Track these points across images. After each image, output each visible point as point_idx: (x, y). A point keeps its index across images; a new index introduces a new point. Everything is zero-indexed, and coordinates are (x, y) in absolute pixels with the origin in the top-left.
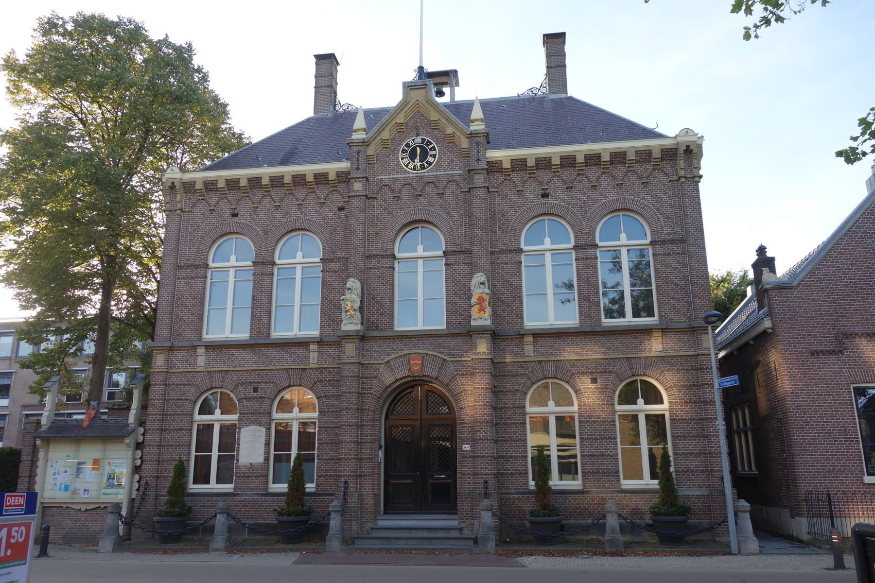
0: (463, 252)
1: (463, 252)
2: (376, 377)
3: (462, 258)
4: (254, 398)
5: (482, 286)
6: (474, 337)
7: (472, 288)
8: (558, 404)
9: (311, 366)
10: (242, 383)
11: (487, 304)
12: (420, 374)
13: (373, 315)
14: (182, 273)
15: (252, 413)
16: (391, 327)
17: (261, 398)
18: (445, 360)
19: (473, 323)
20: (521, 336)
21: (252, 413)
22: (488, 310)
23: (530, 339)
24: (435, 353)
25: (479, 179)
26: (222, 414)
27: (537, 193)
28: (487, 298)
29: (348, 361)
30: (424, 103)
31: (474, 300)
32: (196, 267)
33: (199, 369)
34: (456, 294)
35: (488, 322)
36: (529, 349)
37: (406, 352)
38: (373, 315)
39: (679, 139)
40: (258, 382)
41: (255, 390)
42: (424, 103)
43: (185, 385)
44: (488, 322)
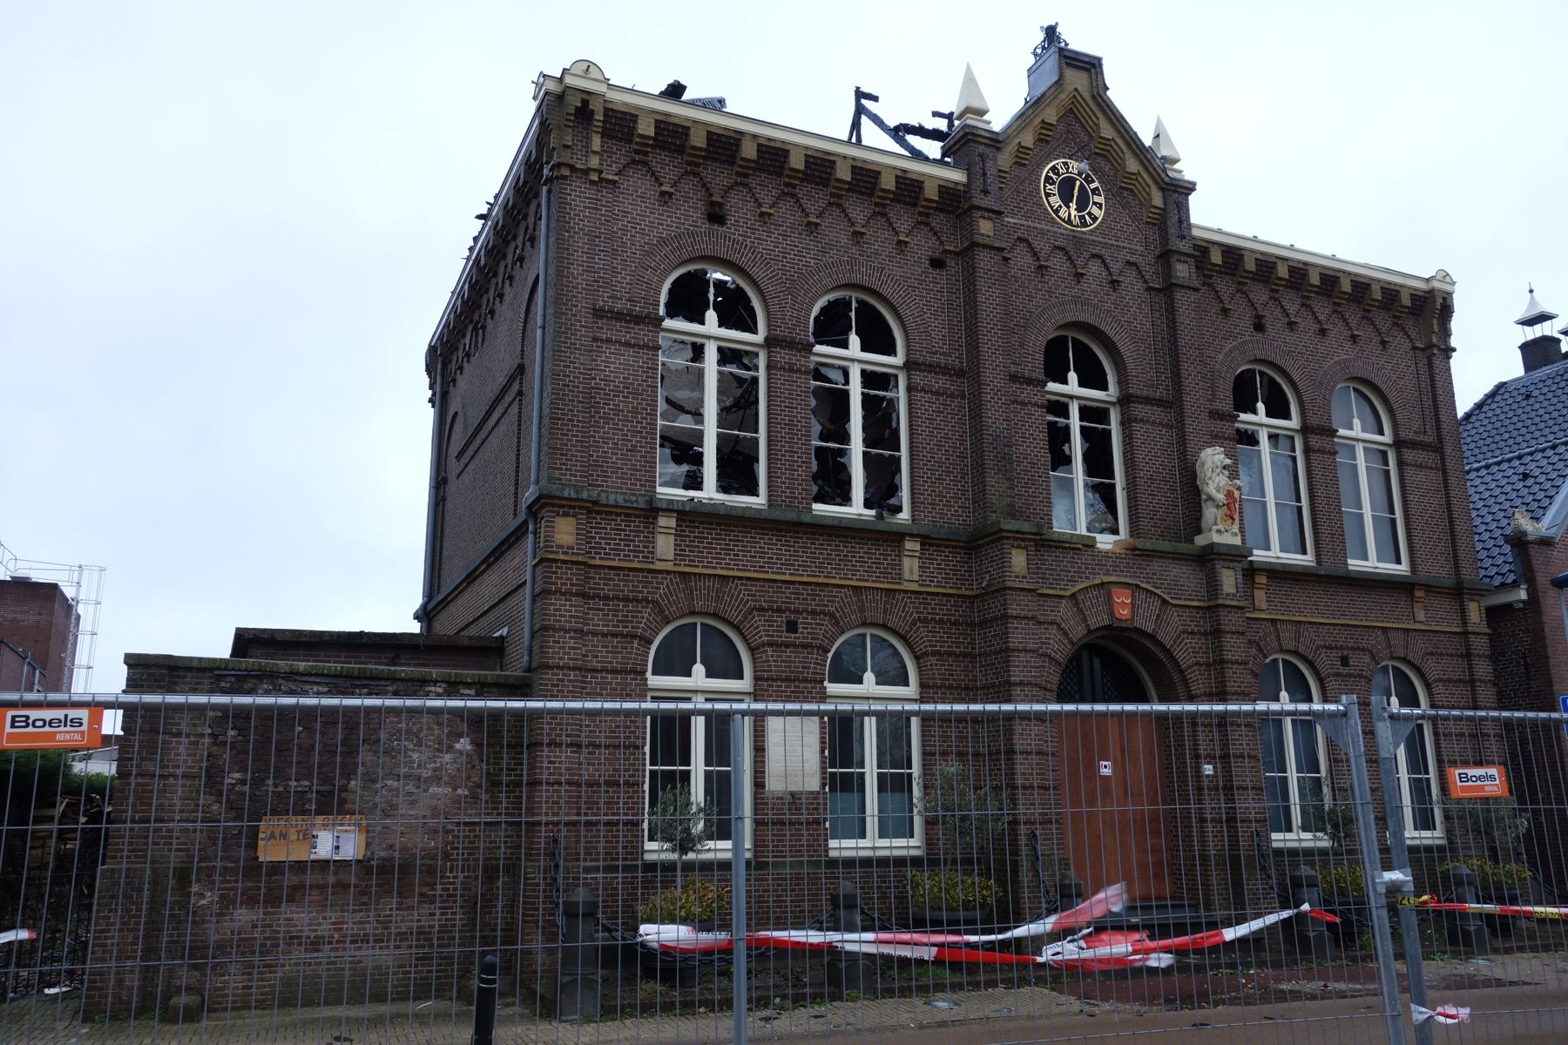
2: (1052, 623)
4: (787, 646)
8: (881, 681)
10: (761, 609)
12: (1129, 625)
14: (607, 330)
15: (787, 679)
17: (804, 646)
18: (1165, 601)
21: (787, 679)
25: (1182, 271)
26: (708, 676)
27: (1246, 322)
30: (1088, 98)
32: (638, 319)
33: (659, 566)
39: (1436, 284)
40: (796, 611)
41: (792, 627)
42: (1088, 98)
43: (626, 600)
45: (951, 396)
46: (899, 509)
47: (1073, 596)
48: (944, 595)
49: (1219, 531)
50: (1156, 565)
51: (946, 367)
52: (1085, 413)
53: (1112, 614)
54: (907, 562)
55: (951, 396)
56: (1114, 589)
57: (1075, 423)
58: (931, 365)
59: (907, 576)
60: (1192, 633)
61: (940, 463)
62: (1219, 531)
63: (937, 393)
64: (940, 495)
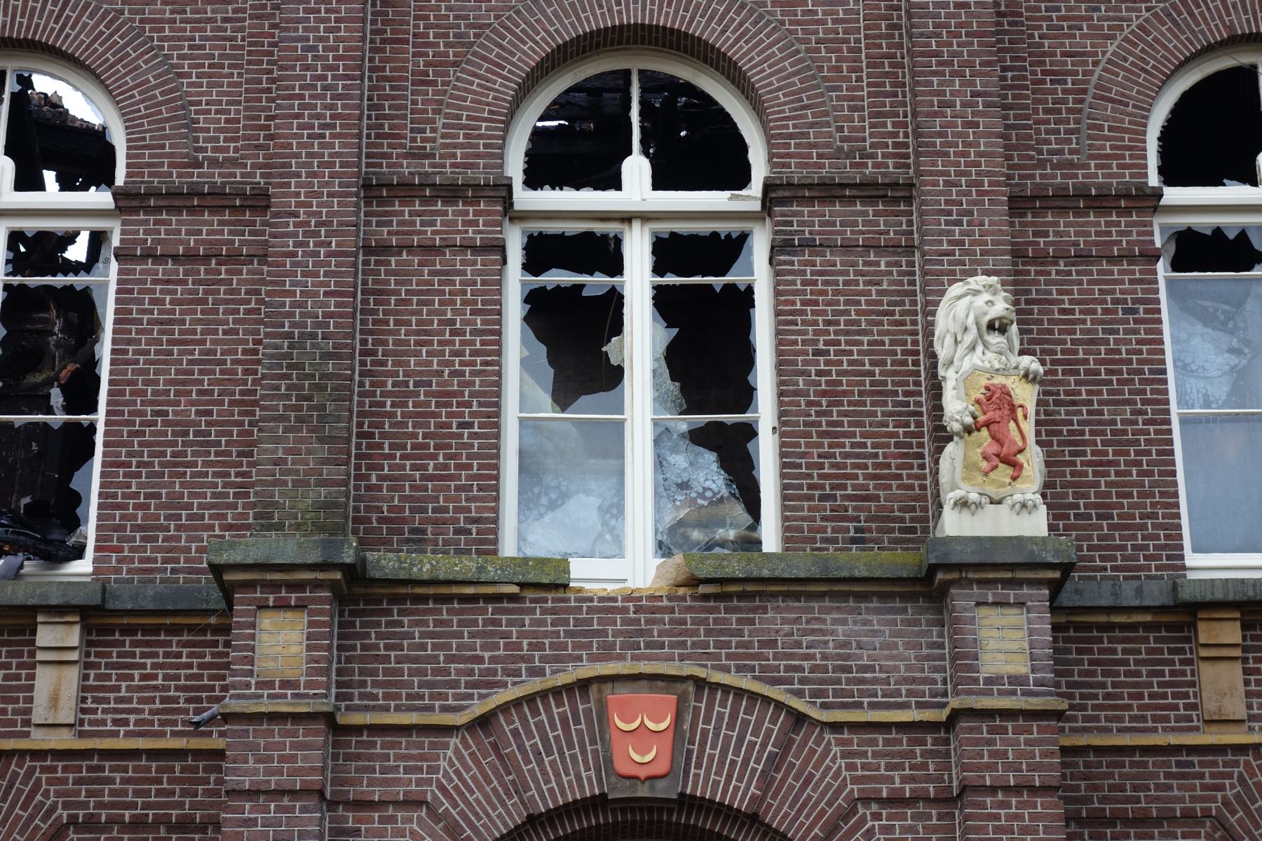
0: (870, 191)
1: (870, 191)
2: (413, 803)
3: (863, 219)
5: (995, 339)
6: (961, 600)
7: (943, 352)
9: (40, 740)
11: (1029, 427)
12: (663, 790)
13: (395, 482)
16: (488, 543)
18: (799, 719)
19: (953, 524)
20: (1185, 613)
22: (1034, 461)
23: (1231, 633)
24: (746, 683)
28: (1026, 395)
29: (265, 706)
31: (956, 407)
34: (833, 393)
35: (1036, 524)
36: (1223, 686)
37: (587, 670)
38: (395, 482)
44: (1036, 524)
45: (234, 258)
46: (78, 553)
47: (484, 722)
48: (153, 754)
49: (963, 504)
50: (776, 620)
51: (217, 193)
52: (669, 253)
53: (606, 763)
54: (44, 680)
55: (234, 258)
56: (617, 697)
57: (638, 280)
58: (174, 194)
59: (40, 713)
60: (896, 800)
61: (182, 428)
62: (963, 504)
63: (191, 257)
64: (175, 503)
